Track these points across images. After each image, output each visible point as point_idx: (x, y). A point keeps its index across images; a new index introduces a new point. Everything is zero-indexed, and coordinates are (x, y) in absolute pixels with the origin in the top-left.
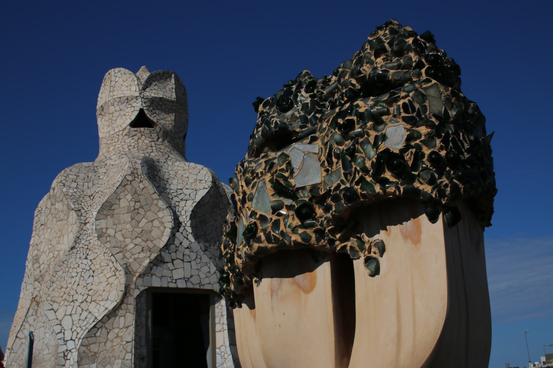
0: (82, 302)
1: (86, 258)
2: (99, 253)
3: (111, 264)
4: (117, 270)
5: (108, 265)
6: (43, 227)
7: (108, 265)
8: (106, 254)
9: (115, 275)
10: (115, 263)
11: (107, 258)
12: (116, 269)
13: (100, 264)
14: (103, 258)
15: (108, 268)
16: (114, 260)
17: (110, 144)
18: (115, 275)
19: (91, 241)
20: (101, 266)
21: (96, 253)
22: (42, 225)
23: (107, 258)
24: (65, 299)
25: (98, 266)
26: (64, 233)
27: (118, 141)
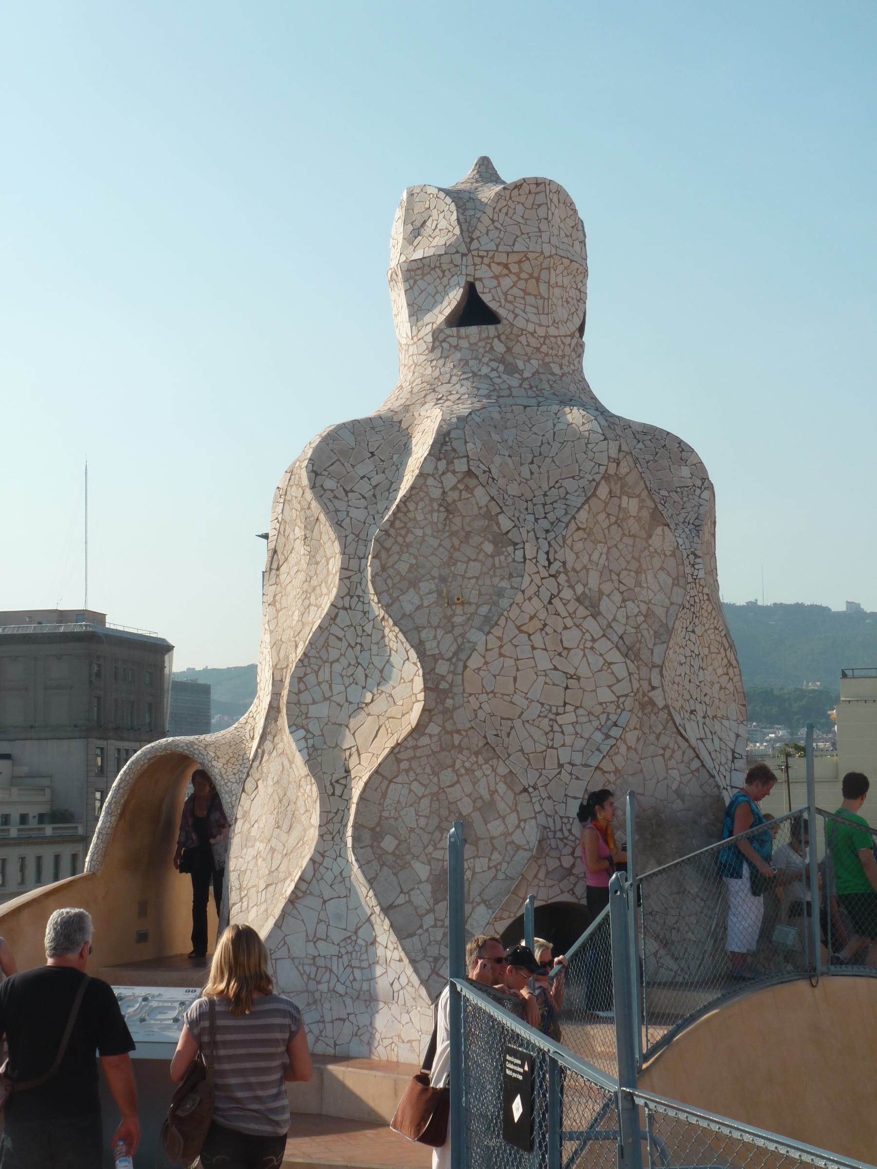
0: (704, 717)
1: (693, 632)
2: (707, 626)
3: (722, 651)
4: (731, 665)
5: (719, 653)
6: (581, 534)
7: (719, 653)
8: (717, 632)
9: (727, 674)
10: (728, 652)
11: (719, 639)
12: (729, 661)
13: (709, 647)
14: (712, 636)
15: (719, 657)
16: (727, 646)
17: (547, 355)
18: (727, 674)
19: (697, 600)
20: (710, 652)
21: (704, 625)
22: (579, 529)
23: (719, 639)
24: (682, 707)
25: (706, 651)
26: (644, 566)
27: (563, 356)
